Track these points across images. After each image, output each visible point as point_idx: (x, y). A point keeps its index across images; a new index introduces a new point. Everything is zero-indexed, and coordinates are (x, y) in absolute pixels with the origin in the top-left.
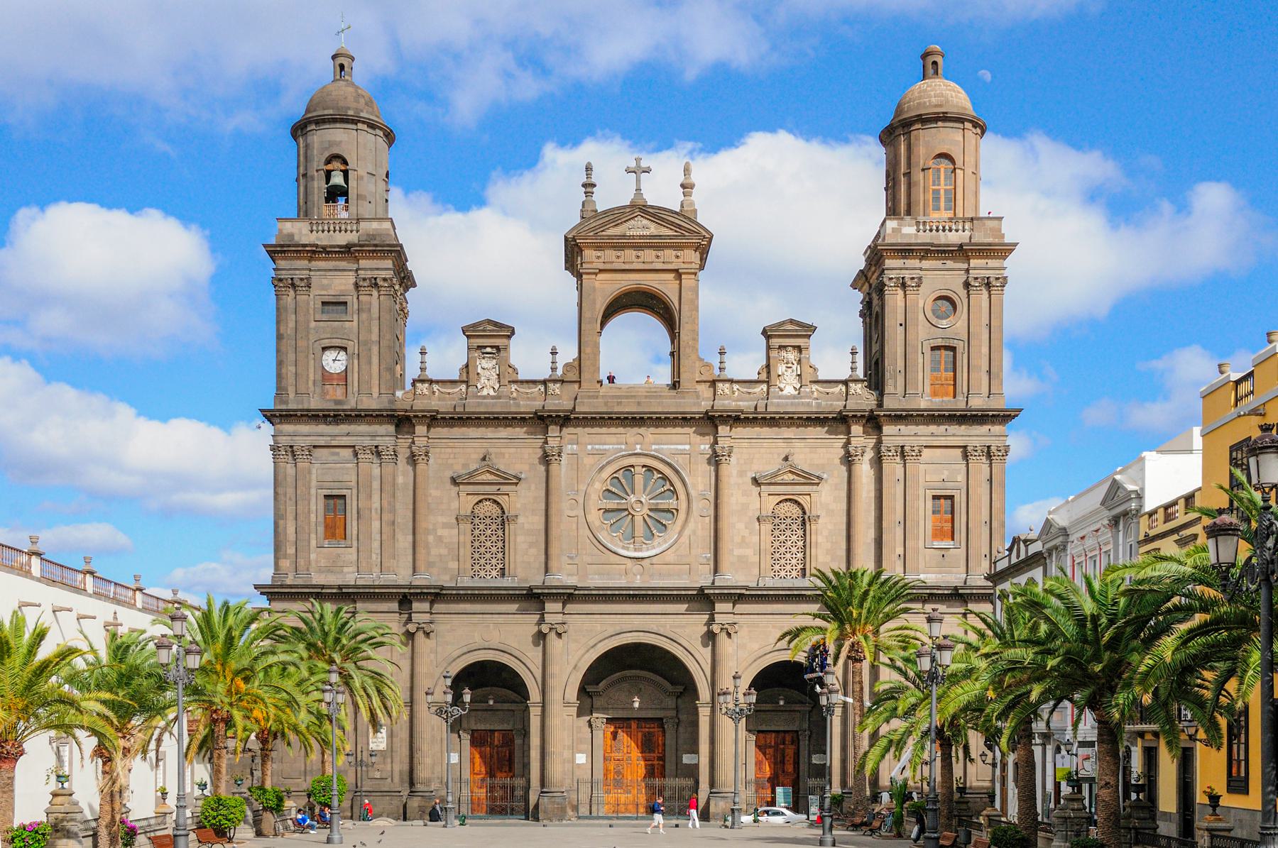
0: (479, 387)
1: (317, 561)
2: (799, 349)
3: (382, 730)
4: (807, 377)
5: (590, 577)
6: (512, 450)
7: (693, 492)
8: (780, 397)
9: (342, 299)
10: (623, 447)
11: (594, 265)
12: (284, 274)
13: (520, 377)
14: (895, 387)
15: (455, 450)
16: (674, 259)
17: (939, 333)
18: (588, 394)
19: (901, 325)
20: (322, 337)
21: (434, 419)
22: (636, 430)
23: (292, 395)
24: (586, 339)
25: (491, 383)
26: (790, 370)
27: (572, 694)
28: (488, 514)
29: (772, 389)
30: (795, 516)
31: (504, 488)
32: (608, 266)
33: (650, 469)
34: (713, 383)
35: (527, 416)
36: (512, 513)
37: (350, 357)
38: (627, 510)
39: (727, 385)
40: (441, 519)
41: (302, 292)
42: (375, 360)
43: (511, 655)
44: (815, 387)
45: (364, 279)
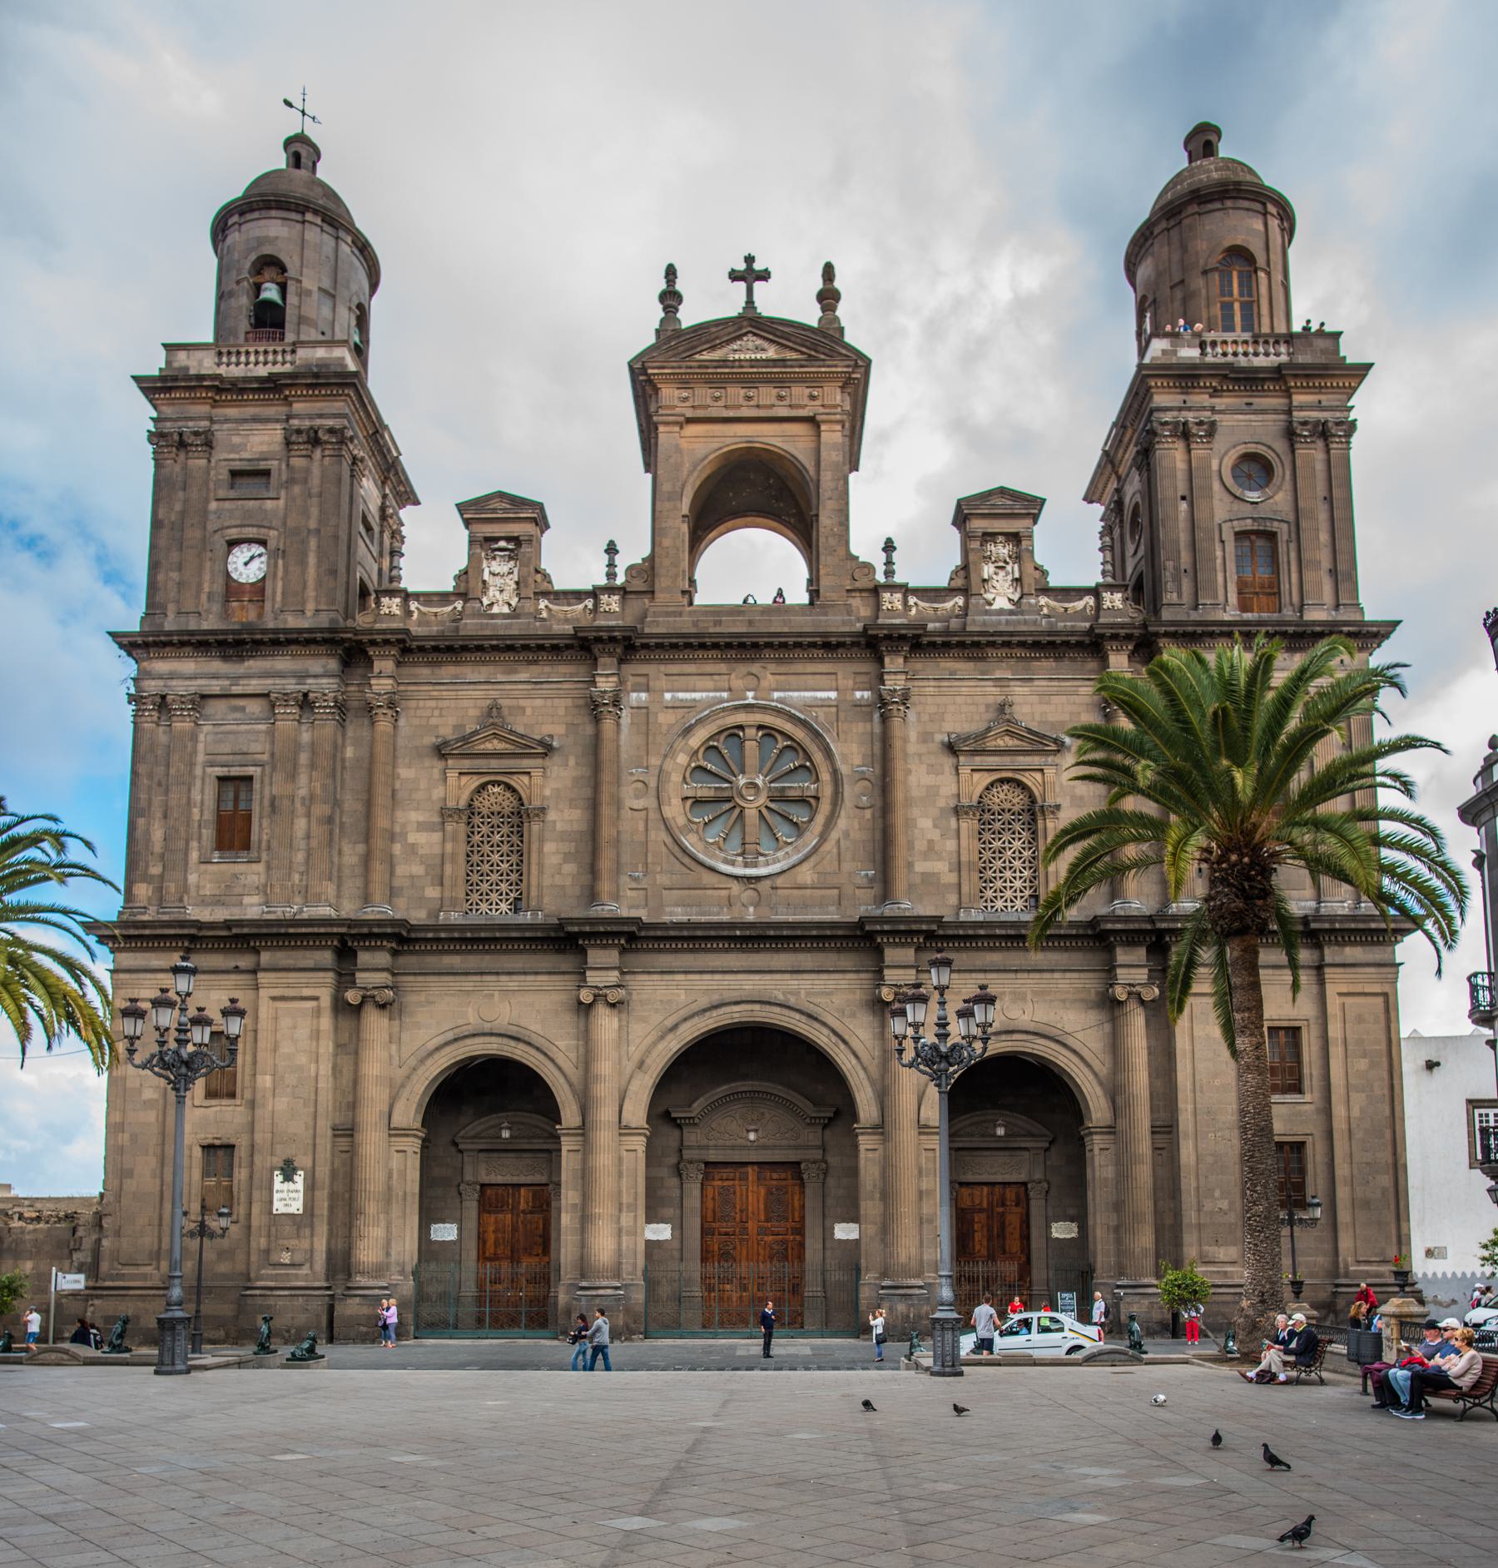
0: (486, 601)
1: (198, 887)
2: (1015, 538)
3: (296, 1178)
4: (1030, 584)
5: (668, 909)
6: (538, 702)
7: (844, 769)
8: (987, 613)
9: (263, 465)
10: (725, 695)
11: (678, 410)
12: (168, 427)
13: (558, 586)
14: (1180, 595)
15: (441, 704)
16: (806, 401)
17: (1247, 510)
18: (665, 609)
19: (1183, 498)
20: (227, 524)
21: (408, 648)
22: (743, 668)
23: (171, 616)
24: (664, 525)
25: (506, 596)
26: (1002, 573)
27: (637, 1112)
28: (496, 808)
29: (973, 600)
30: (1016, 808)
31: (526, 763)
32: (700, 413)
33: (769, 732)
34: (876, 590)
35: (562, 642)
36: (536, 803)
37: (274, 555)
38: (729, 800)
39: (899, 596)
40: (415, 816)
41: (196, 454)
42: (312, 560)
43: (529, 1044)
44: (1043, 600)
45: (299, 432)
